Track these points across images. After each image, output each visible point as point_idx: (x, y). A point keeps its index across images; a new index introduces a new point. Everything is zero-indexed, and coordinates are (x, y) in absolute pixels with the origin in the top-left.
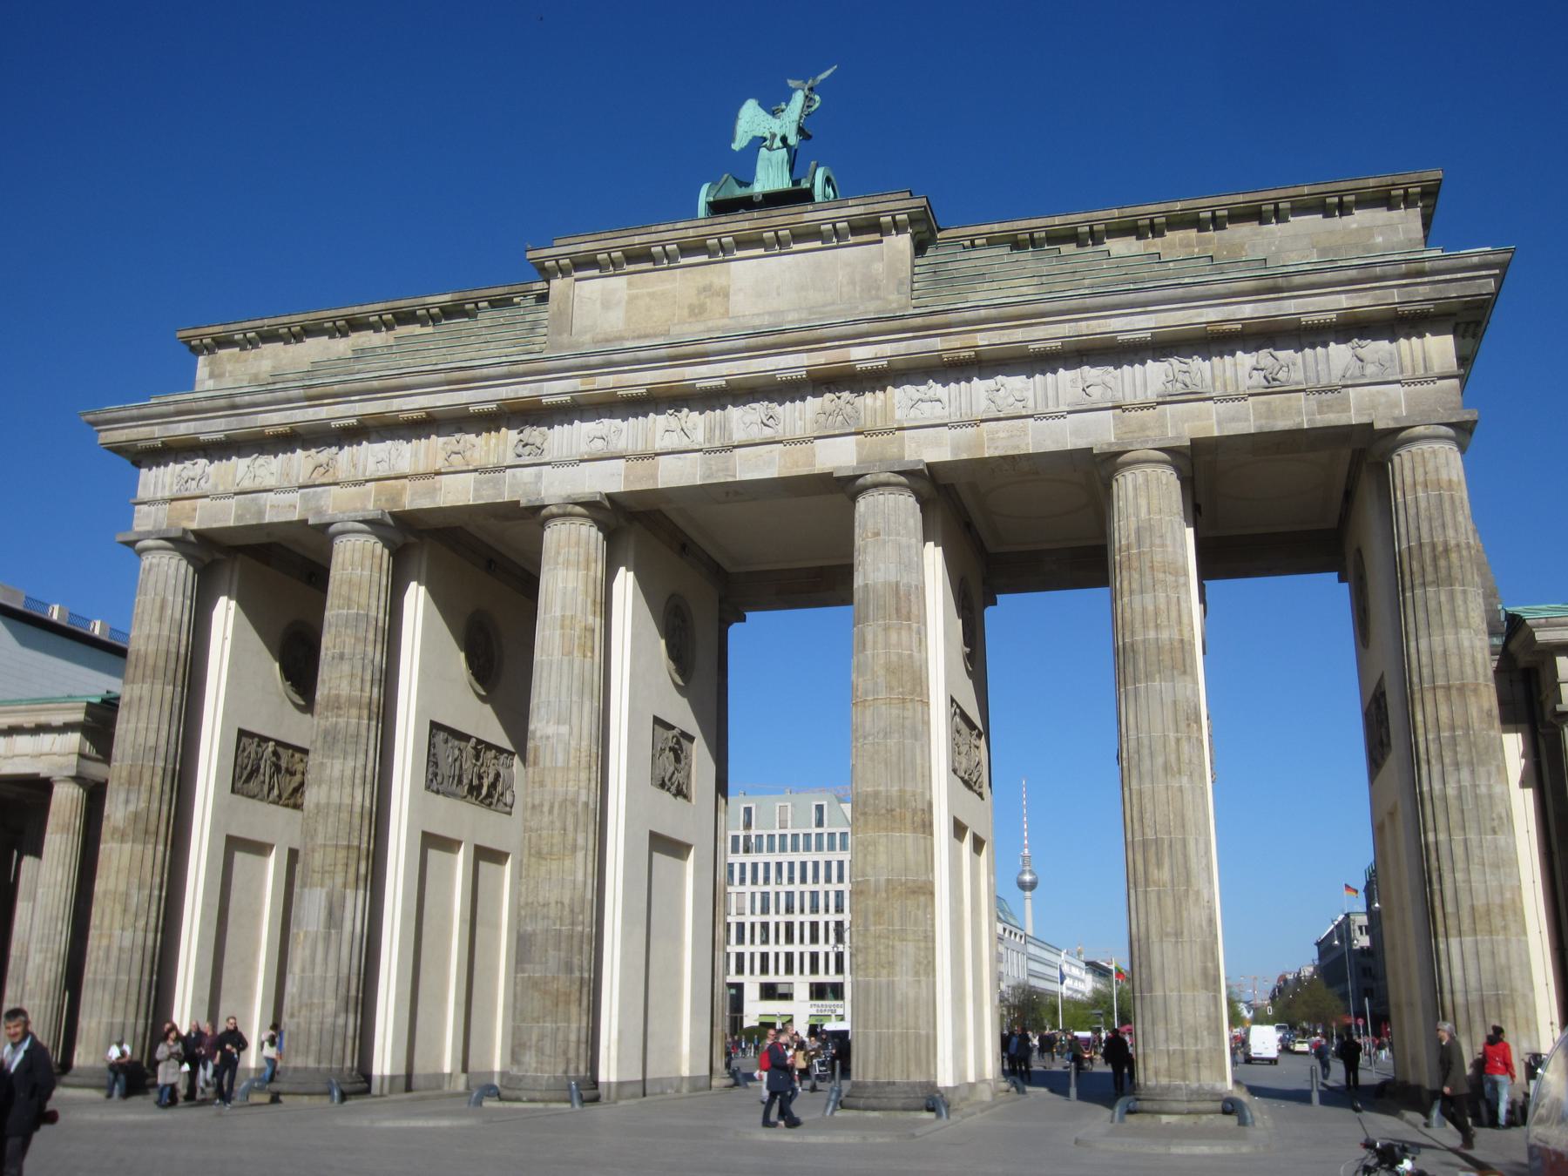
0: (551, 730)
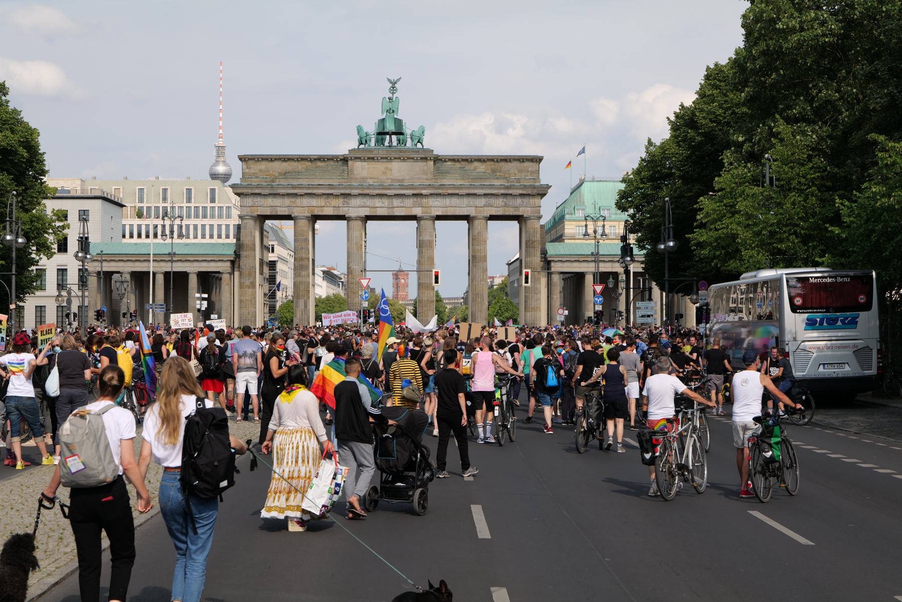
0: (354, 267)
